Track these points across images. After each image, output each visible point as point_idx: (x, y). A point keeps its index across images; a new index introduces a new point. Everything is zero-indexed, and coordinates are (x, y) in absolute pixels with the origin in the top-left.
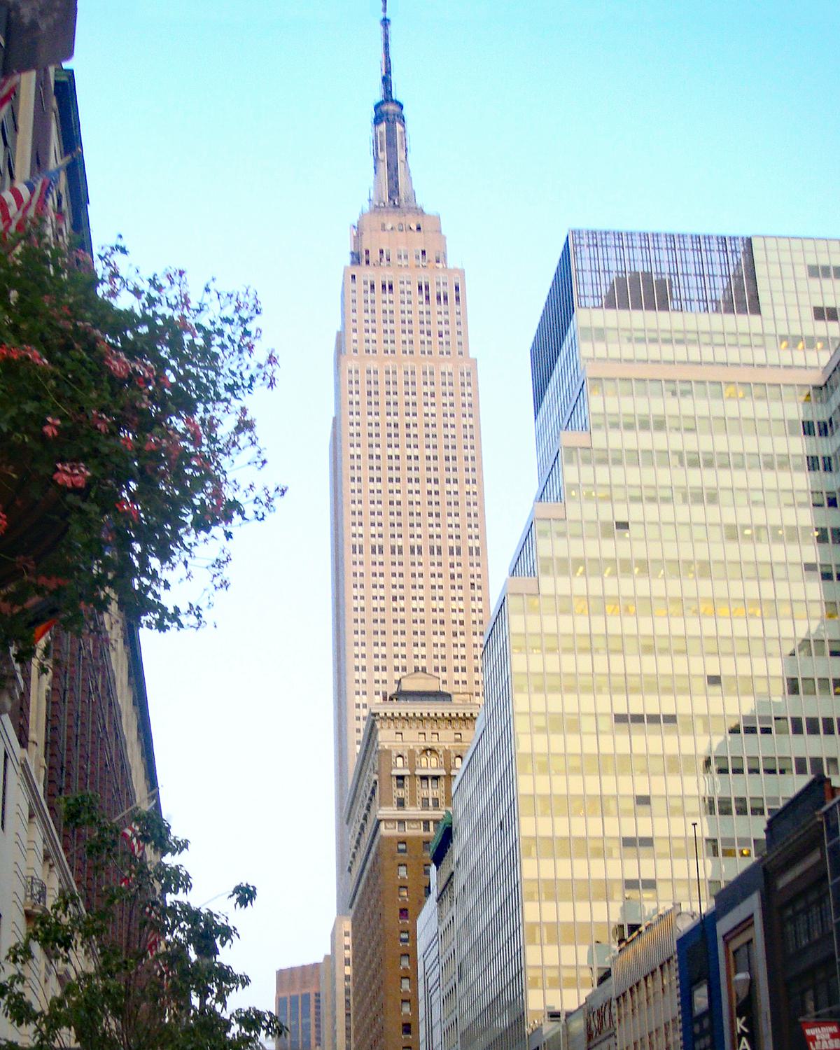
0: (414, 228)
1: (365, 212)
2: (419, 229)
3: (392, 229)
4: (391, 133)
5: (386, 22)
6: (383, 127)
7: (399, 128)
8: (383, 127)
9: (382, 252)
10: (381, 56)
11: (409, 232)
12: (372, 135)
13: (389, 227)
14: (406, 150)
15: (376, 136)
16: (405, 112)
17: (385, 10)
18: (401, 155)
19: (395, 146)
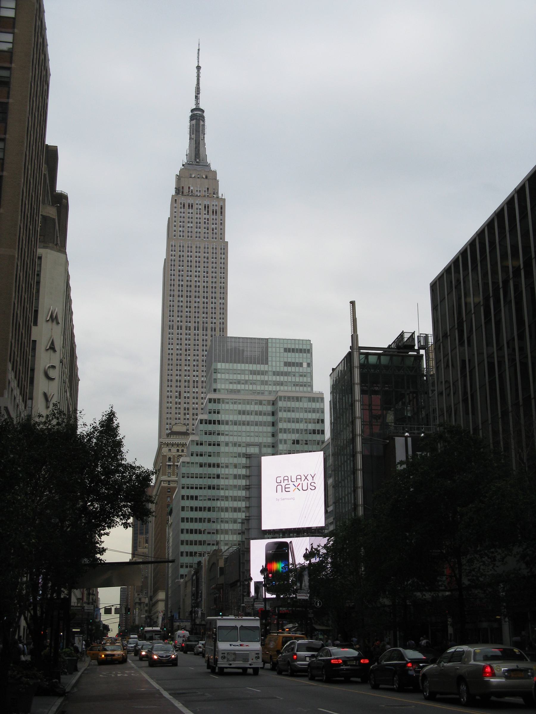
0: (204, 177)
1: (184, 163)
2: (206, 177)
3: (194, 177)
4: (198, 125)
5: (199, 68)
6: (194, 122)
7: (201, 123)
8: (194, 122)
9: (189, 188)
10: (196, 83)
11: (202, 179)
12: (189, 124)
13: (193, 176)
14: (204, 134)
15: (190, 126)
16: (205, 114)
17: (198, 62)
18: (201, 137)
19: (199, 132)
